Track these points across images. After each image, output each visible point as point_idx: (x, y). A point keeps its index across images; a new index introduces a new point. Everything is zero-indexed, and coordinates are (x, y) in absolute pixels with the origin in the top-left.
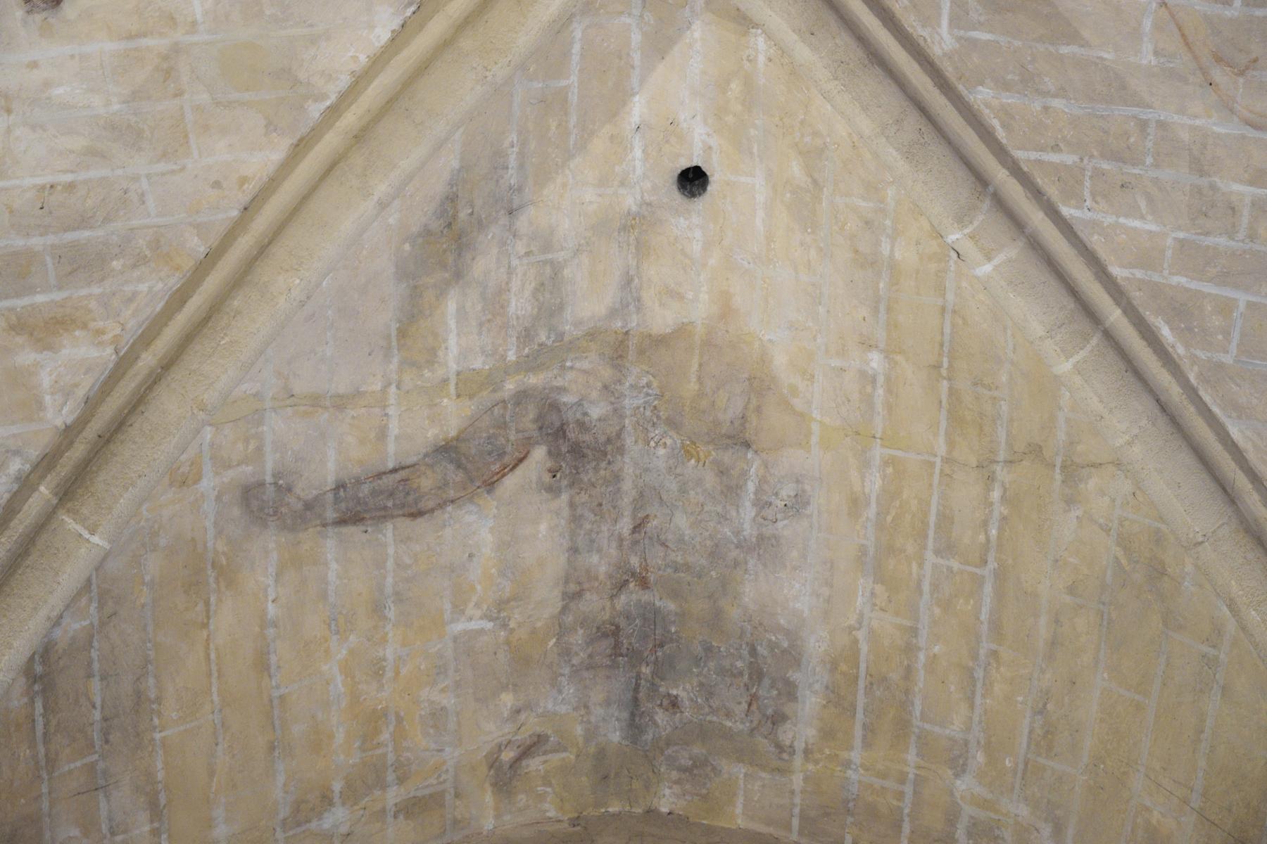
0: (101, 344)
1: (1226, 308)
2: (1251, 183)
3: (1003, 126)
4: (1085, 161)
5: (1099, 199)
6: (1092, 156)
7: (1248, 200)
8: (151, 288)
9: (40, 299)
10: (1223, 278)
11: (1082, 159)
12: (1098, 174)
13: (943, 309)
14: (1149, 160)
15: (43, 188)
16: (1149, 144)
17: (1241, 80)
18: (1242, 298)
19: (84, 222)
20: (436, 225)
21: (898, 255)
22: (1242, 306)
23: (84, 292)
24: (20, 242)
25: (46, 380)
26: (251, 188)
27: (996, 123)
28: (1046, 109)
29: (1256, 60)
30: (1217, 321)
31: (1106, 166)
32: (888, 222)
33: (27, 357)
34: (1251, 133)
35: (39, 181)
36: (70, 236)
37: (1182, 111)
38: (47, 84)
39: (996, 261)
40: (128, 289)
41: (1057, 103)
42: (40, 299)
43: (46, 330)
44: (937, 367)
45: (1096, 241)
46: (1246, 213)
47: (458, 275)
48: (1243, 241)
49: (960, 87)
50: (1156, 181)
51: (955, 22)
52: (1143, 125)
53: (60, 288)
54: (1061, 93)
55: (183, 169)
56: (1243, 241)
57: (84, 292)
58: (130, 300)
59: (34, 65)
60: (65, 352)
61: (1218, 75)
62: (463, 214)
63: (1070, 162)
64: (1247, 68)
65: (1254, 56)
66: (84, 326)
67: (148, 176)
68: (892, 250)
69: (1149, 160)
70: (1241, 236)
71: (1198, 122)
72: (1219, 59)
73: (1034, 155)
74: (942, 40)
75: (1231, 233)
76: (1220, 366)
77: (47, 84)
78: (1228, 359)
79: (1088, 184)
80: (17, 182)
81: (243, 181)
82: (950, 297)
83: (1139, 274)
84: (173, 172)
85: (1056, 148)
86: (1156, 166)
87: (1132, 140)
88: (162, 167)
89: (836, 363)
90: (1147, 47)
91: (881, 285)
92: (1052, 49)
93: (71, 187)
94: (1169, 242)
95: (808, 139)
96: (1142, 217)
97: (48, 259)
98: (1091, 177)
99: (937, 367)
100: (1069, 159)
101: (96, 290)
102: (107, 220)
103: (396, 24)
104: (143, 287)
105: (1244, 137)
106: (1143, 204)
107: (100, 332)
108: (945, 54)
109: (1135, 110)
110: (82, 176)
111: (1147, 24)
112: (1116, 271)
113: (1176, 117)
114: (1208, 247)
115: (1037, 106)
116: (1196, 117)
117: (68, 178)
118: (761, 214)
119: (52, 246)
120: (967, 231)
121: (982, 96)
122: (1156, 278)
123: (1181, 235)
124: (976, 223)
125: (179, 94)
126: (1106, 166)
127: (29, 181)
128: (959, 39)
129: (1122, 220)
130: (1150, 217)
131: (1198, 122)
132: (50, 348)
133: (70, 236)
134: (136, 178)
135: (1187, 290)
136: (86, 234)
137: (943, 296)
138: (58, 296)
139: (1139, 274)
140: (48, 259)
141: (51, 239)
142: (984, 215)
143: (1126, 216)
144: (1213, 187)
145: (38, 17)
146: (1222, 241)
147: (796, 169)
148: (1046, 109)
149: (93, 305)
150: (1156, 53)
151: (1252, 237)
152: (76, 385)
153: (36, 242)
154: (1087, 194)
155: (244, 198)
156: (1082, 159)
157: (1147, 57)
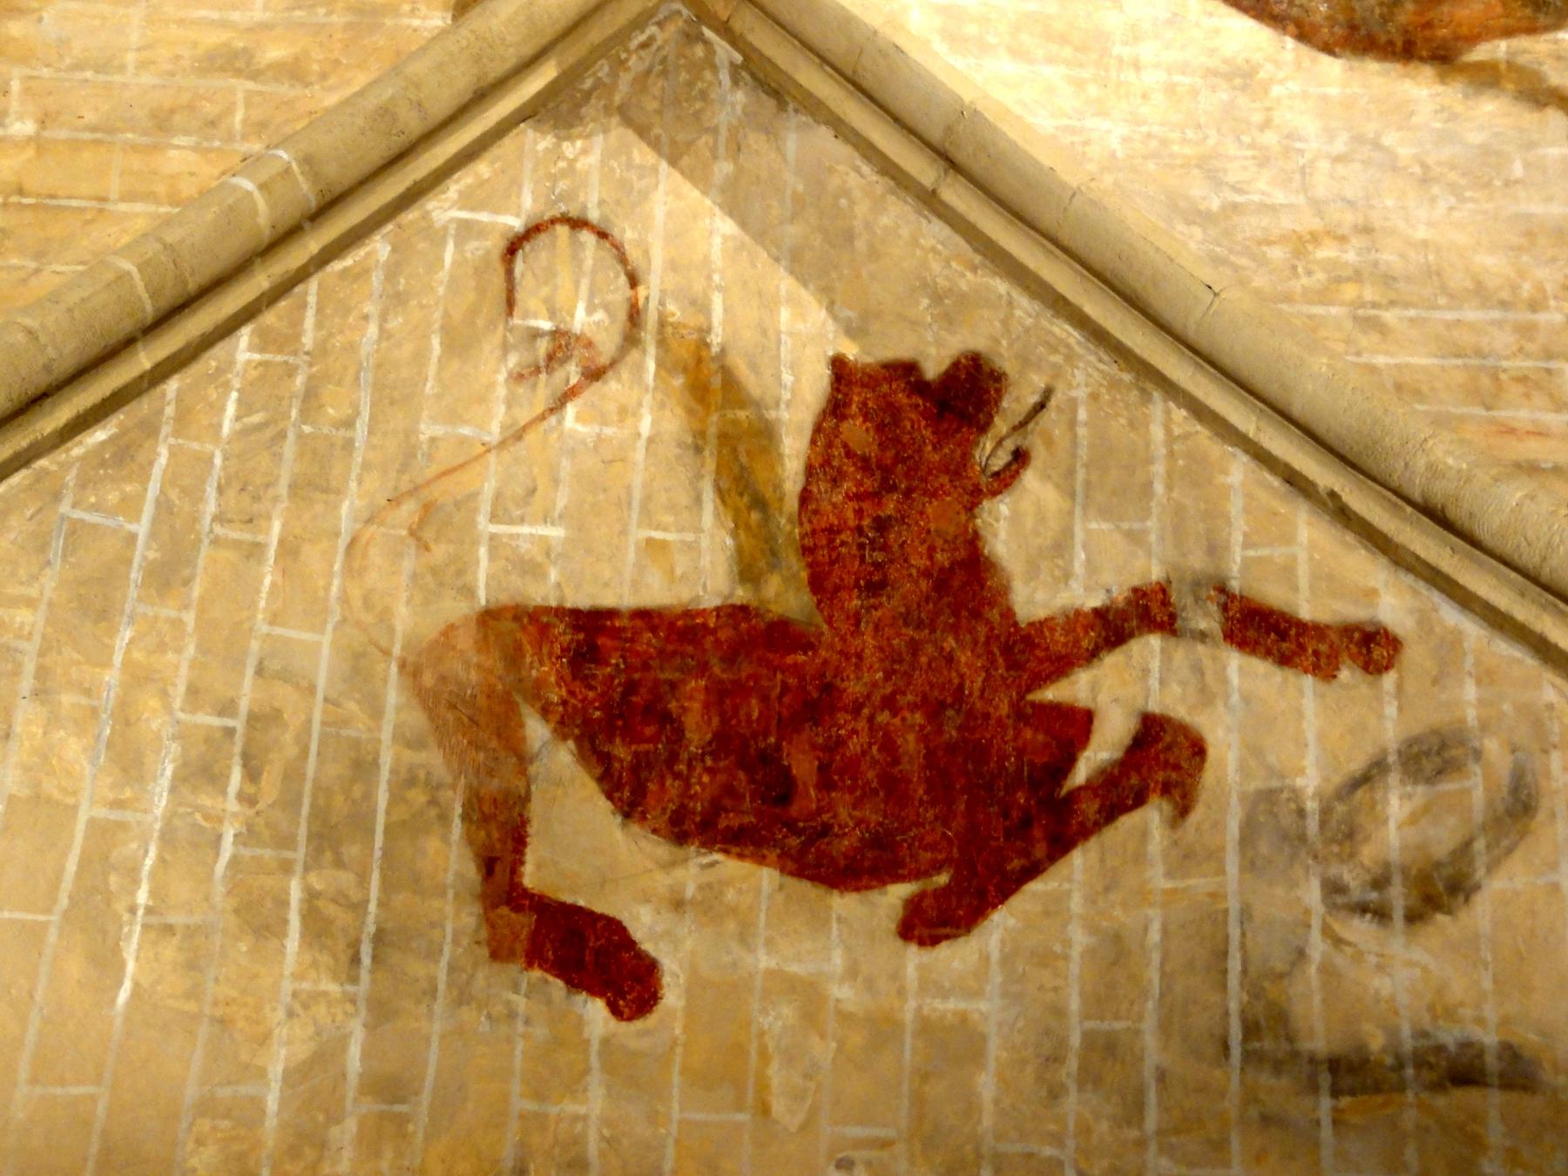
1: (131, 506)
2: (281, 542)
3: (346, 270)
4: (306, 358)
5: (261, 369)
6: (311, 365)
7: (260, 538)
10: (164, 507)
11: (307, 353)
12: (291, 371)
13: (103, 199)
14: (307, 429)
16: (325, 431)
17: (404, 533)
18: (142, 528)
21: (173, 153)
22: (132, 527)
27: (349, 261)
28: (366, 318)
29: (427, 549)
30: (113, 497)
31: (299, 381)
32: (217, 143)
34: (342, 543)
37: (366, 466)
39: (257, 194)
41: (372, 330)
44: (21, 192)
45: (210, 361)
46: (247, 537)
48: (211, 531)
49: (390, 227)
50: (282, 435)
51: (466, 230)
52: (349, 423)
54: (384, 334)
56: (211, 531)
61: (409, 509)
63: (304, 340)
64: (419, 539)
65: (433, 546)
68: (178, 147)
69: (307, 429)
70: (218, 529)
71: (353, 485)
72: (428, 509)
73: (312, 299)
74: (443, 208)
75: (219, 518)
76: (57, 497)
78: (65, 508)
79: (279, 358)
82: (123, 207)
83: (170, 411)
85: (319, 325)
86: (301, 436)
87: (331, 411)
89: (15, 86)
90: (439, 430)
91: (130, 135)
92: (437, 326)
94: (209, 447)
95: (316, 67)
96: (238, 418)
98: (286, 363)
99: (21, 192)
100: (308, 340)
105: (337, 535)
106: (256, 418)
108: (428, 213)
109: (365, 415)
111: (466, 431)
112: (172, 386)
113: (360, 460)
114: (204, 491)
115: (370, 308)
116: (360, 483)
118: (215, 15)
120: (294, 166)
121: (379, 247)
122: (165, 430)
123: (218, 461)
124: (301, 178)
126: (299, 381)
128: (445, 228)
129: (234, 395)
130: (238, 426)
131: (353, 485)
135: (151, 463)
137: (123, 199)
139: (170, 411)
142: (306, 192)
143: (239, 401)
144: (276, 499)
146: (211, 507)
147: (274, 52)
148: (366, 318)
150: (433, 440)
151: (216, 542)
154: (267, 357)
156: (307, 353)
157: (427, 430)
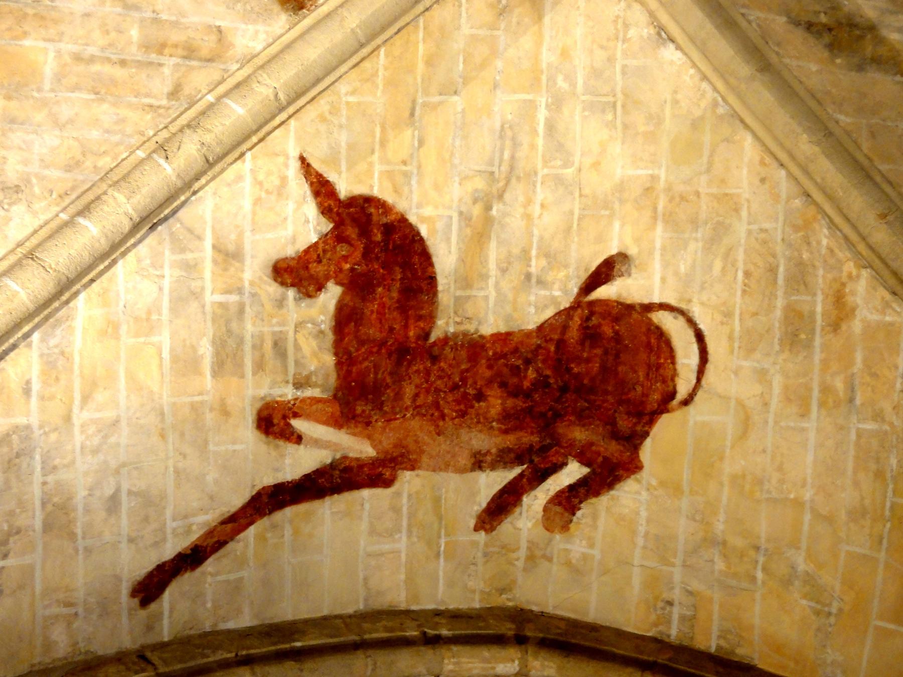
0: (858, 276)
8: (826, 236)
9: (819, 309)
15: (744, 291)
19: (773, 270)
20: (827, 39)
23: (820, 281)
24: (778, 313)
25: (875, 317)
26: (768, 160)
33: (857, 326)
35: (739, 293)
36: (781, 281)
38: (676, 273)
40: (824, 251)
42: (819, 309)
43: (841, 310)
47: (872, 28)
53: (815, 295)
55: (748, 201)
57: (820, 281)
58: (832, 251)
59: (663, 280)
60: (859, 301)
62: (823, 19)
66: (844, 285)
67: (749, 223)
77: (676, 273)
80: (738, 306)
81: (762, 163)
84: (749, 208)
88: (744, 213)
93: (747, 274)
97: (794, 298)
101: (821, 272)
102: (774, 256)
103: (671, 46)
104: (825, 242)
107: (850, 276)
110: (741, 265)
117: (740, 275)
119: (785, 293)
125: (698, 194)
127: (738, 300)
132: (853, 310)
133: (781, 281)
134: (749, 232)
136: (781, 269)
138: (820, 298)
140: (794, 298)
141: (780, 293)
145: (633, 270)
149: (830, 276)
152: (883, 298)
153: (780, 303)
155: (775, 164)
